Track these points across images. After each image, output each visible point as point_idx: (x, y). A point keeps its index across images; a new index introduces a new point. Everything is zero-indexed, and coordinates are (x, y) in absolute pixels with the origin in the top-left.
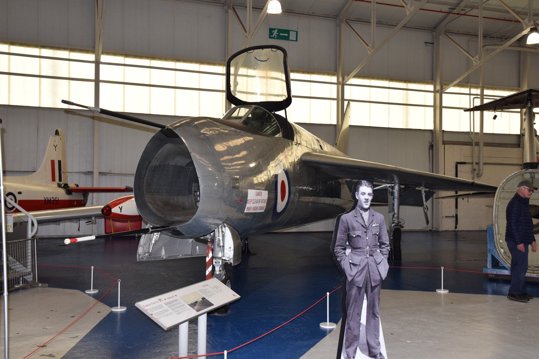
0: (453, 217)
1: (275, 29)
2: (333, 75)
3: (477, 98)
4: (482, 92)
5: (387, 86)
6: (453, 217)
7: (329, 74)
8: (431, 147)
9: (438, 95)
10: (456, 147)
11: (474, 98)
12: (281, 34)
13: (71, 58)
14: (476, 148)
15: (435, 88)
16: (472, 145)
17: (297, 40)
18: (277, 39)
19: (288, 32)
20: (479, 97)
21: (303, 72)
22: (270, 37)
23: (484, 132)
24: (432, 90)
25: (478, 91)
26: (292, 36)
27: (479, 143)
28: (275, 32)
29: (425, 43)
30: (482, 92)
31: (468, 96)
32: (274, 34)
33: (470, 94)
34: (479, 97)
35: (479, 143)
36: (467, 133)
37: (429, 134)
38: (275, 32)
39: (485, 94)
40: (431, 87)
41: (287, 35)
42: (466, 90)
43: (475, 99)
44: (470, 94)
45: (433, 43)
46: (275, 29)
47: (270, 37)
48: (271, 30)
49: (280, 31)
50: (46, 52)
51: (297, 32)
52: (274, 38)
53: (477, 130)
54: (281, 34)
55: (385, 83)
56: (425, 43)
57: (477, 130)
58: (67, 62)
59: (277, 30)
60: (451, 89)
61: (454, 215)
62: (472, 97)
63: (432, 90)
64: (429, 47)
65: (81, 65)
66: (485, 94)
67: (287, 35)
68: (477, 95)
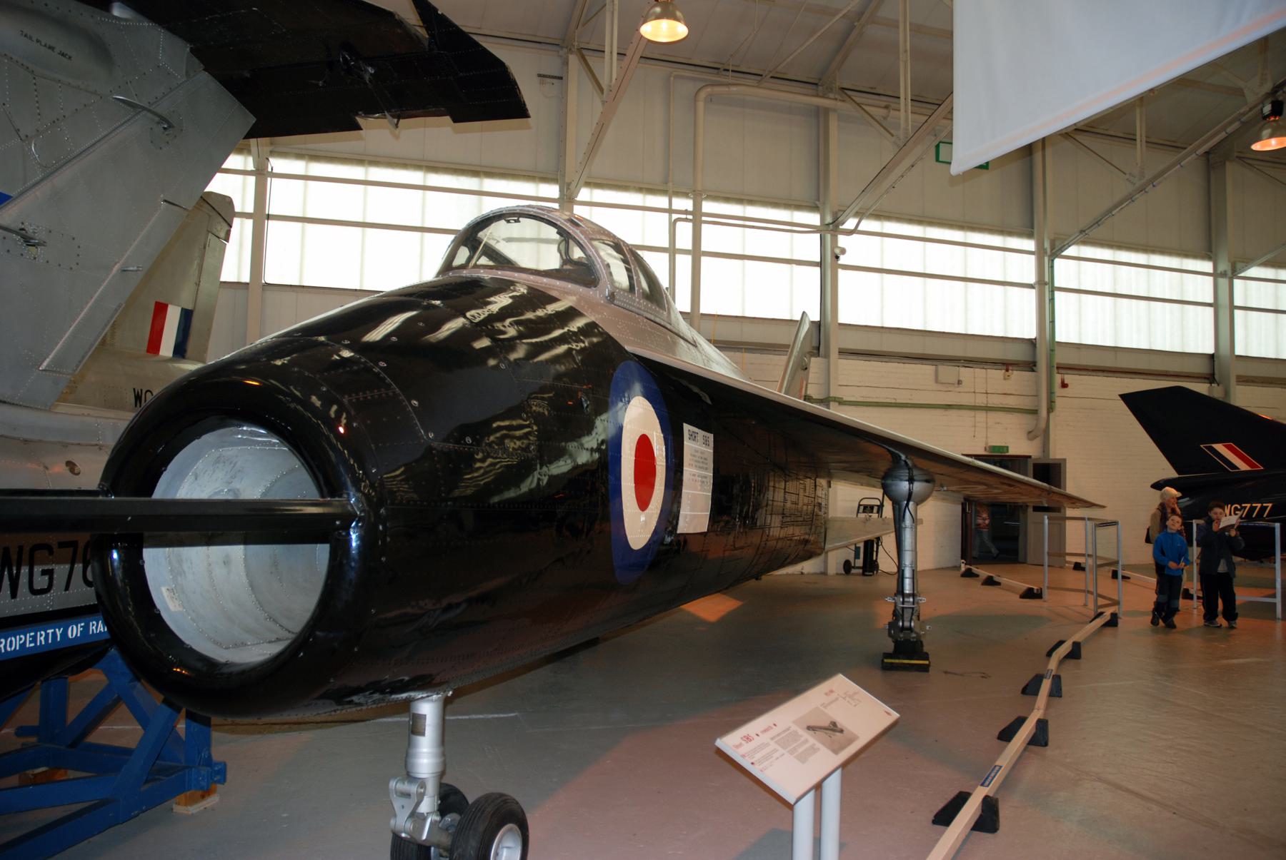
3: (686, 220)
4: (697, 206)
20: (690, 217)
23: (703, 310)
25: (685, 204)
29: (540, 75)
30: (697, 206)
33: (670, 211)
34: (690, 217)
39: (704, 210)
42: (661, 201)
43: (679, 224)
44: (670, 211)
55: (415, 177)
56: (540, 75)
62: (675, 216)
66: (704, 210)
68: (686, 212)
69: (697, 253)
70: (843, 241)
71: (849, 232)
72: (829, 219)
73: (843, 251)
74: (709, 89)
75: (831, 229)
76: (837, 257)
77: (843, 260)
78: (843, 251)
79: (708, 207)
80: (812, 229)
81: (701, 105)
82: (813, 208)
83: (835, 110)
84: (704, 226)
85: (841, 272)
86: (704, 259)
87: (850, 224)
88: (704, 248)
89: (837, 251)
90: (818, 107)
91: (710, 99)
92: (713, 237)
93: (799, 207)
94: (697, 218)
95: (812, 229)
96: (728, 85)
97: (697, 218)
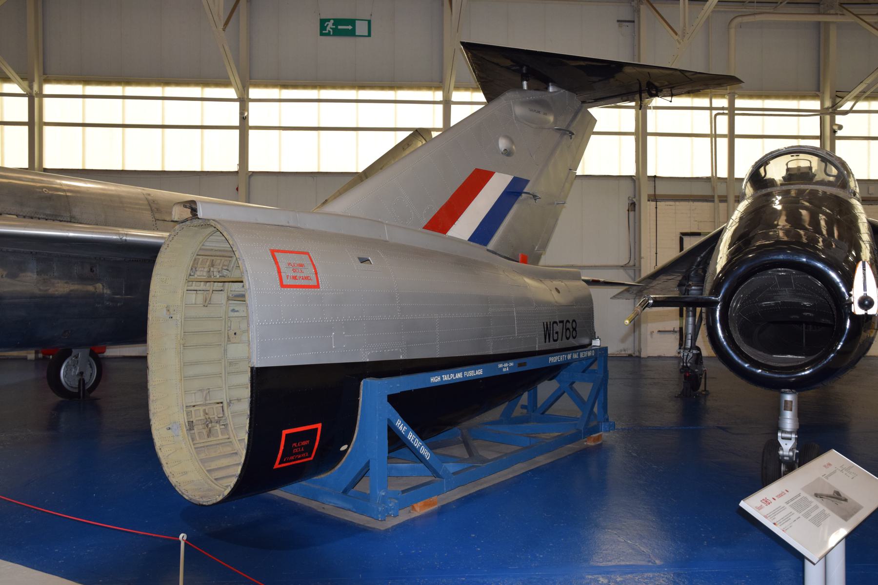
0: (674, 331)
1: (329, 20)
2: (437, 88)
3: (723, 114)
5: (277, 97)
6: (674, 331)
7: (429, 88)
8: (633, 206)
9: (828, 118)
10: (683, 206)
11: (716, 115)
12: (340, 27)
13: (126, 94)
14: (723, 206)
15: (822, 104)
16: (713, 201)
17: (369, 35)
18: (334, 35)
19: (352, 22)
20: (726, 112)
21: (382, 88)
22: (322, 34)
24: (819, 108)
25: (723, 102)
26: (361, 28)
27: (726, 197)
28: (330, 25)
29: (618, 21)
31: (708, 111)
32: (328, 28)
33: (711, 108)
34: (726, 112)
35: (726, 197)
36: (708, 179)
37: (629, 183)
38: (330, 25)
40: (815, 105)
41: (350, 27)
42: (704, 102)
43: (718, 117)
44: (711, 108)
45: (633, 22)
46: (329, 20)
47: (322, 34)
48: (323, 22)
49: (337, 22)
50: (131, 90)
51: (369, 22)
52: (328, 34)
53: (723, 173)
54: (340, 27)
56: (618, 21)
57: (723, 173)
58: (81, 100)
59: (332, 21)
60: (657, 101)
61: (677, 329)
62: (715, 112)
63: (819, 108)
64: (627, 29)
65: (218, 106)
67: (350, 27)
68: (723, 108)
69: (732, 136)
70: (839, 119)
71: (845, 113)
72: (828, 104)
73: (840, 127)
74: (739, 20)
75: (830, 112)
76: (835, 132)
77: (839, 133)
78: (840, 127)
79: (739, 103)
80: (813, 112)
81: (732, 31)
82: (814, 97)
83: (833, 22)
84: (736, 117)
85: (837, 142)
86: (736, 140)
87: (847, 106)
88: (736, 133)
89: (835, 128)
90: (819, 23)
91: (741, 25)
92: (743, 124)
93: (803, 97)
94: (732, 112)
95: (813, 112)
96: (754, 14)
97: (732, 112)
